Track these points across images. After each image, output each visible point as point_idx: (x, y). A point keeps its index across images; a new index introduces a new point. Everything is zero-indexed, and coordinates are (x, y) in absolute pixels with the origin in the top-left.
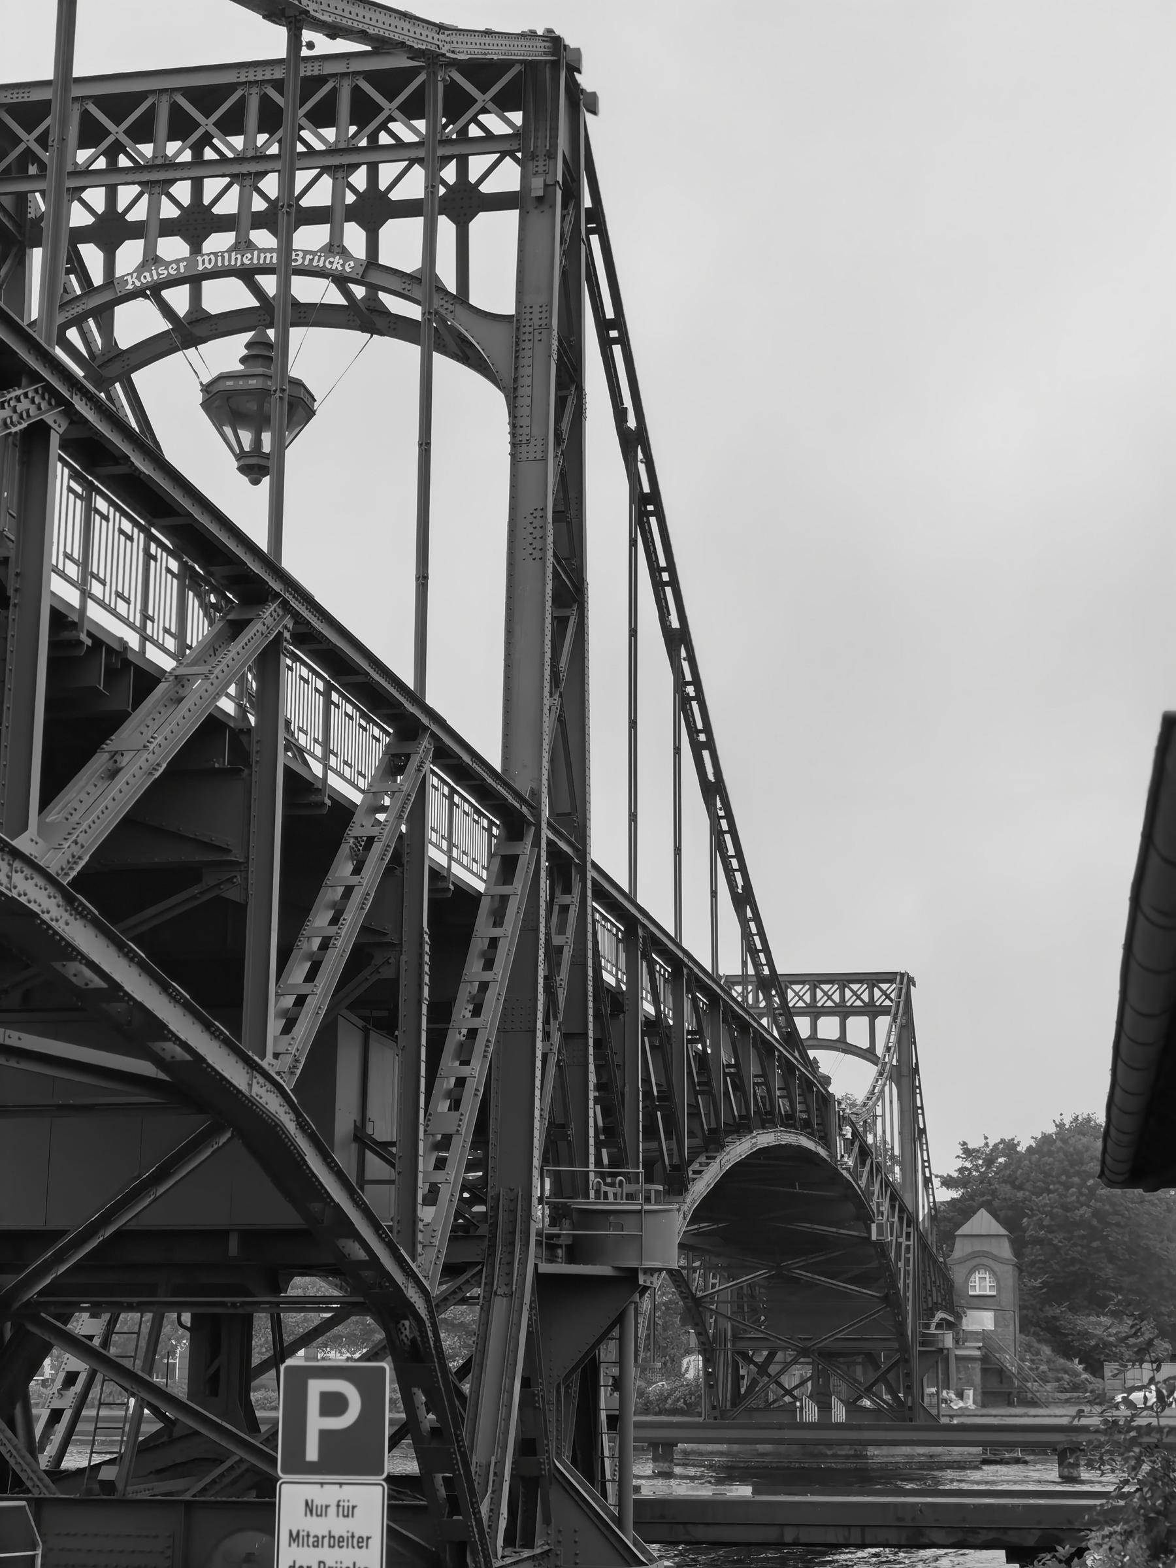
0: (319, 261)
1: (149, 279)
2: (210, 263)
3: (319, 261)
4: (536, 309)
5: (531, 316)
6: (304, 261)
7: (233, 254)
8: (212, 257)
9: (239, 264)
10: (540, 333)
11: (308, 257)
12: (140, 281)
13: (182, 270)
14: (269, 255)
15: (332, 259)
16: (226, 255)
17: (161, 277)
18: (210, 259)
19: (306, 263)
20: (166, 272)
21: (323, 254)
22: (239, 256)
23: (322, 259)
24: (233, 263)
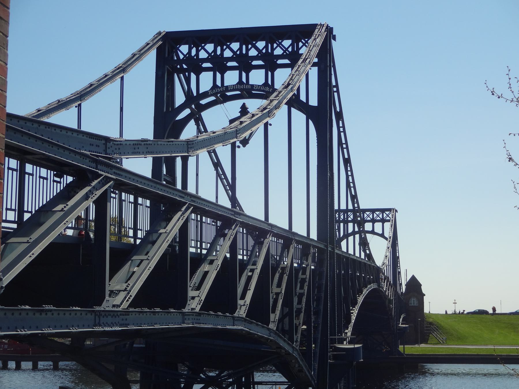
0: (262, 88)
1: (215, 92)
2: (232, 88)
3: (262, 88)
6: (258, 88)
9: (240, 88)
11: (259, 87)
12: (212, 92)
13: (224, 89)
15: (266, 88)
16: (236, 85)
18: (232, 87)
19: (259, 89)
20: (219, 90)
22: (240, 86)
23: (263, 87)
24: (238, 88)
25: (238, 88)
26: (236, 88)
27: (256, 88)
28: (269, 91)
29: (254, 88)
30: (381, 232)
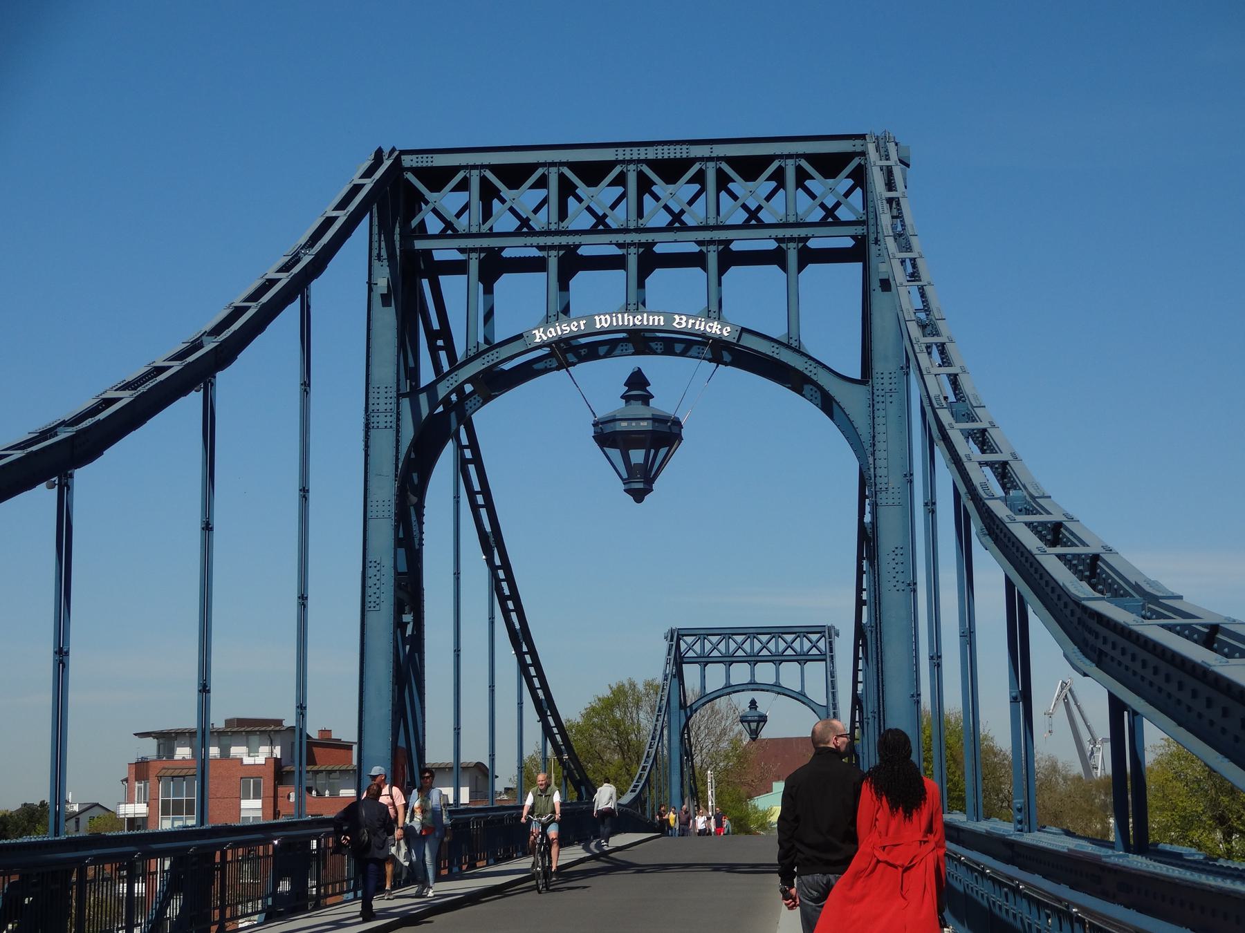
0: (700, 325)
1: (555, 335)
2: (606, 323)
3: (700, 325)
4: (886, 376)
5: (882, 381)
6: (687, 324)
7: (626, 315)
8: (607, 316)
9: (631, 324)
10: (891, 396)
12: (546, 335)
13: (583, 328)
14: (656, 318)
15: (711, 324)
16: (620, 316)
17: (565, 332)
19: (690, 326)
20: (568, 328)
21: (703, 320)
22: (631, 318)
23: (703, 323)
24: (626, 323)
25: (626, 323)
26: (620, 323)
27: (679, 324)
28: (722, 333)
29: (675, 324)
30: (798, 689)
